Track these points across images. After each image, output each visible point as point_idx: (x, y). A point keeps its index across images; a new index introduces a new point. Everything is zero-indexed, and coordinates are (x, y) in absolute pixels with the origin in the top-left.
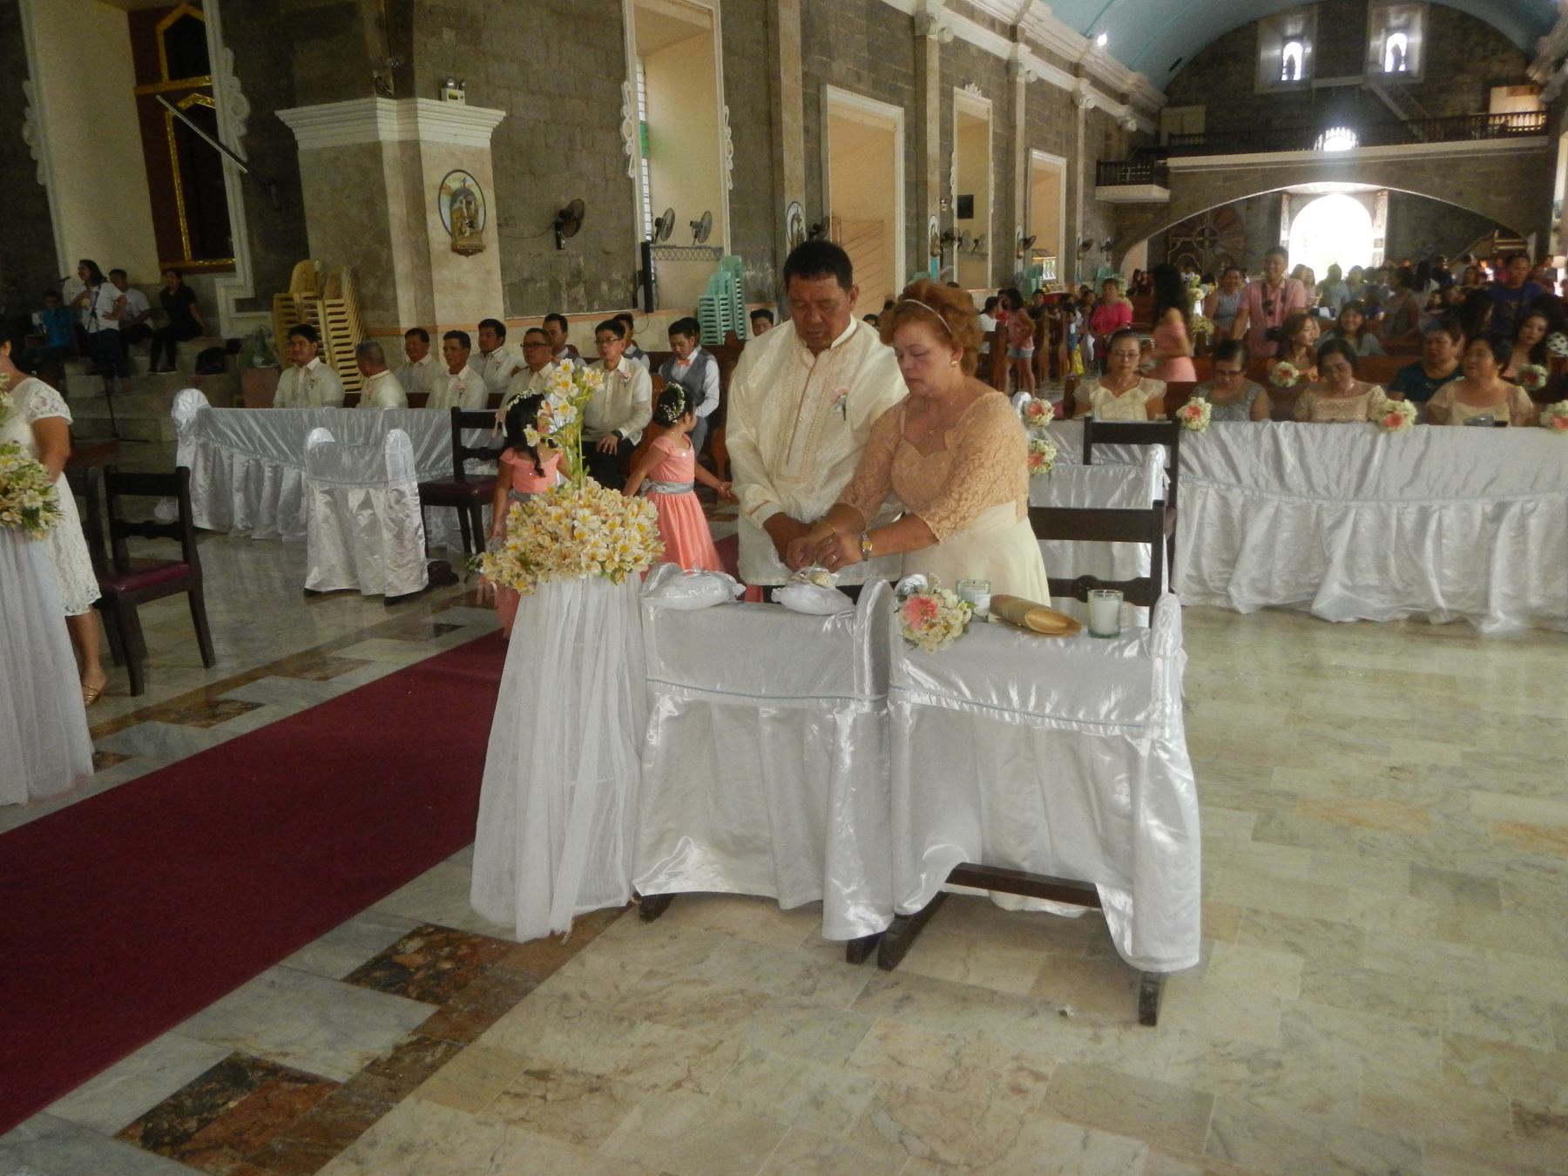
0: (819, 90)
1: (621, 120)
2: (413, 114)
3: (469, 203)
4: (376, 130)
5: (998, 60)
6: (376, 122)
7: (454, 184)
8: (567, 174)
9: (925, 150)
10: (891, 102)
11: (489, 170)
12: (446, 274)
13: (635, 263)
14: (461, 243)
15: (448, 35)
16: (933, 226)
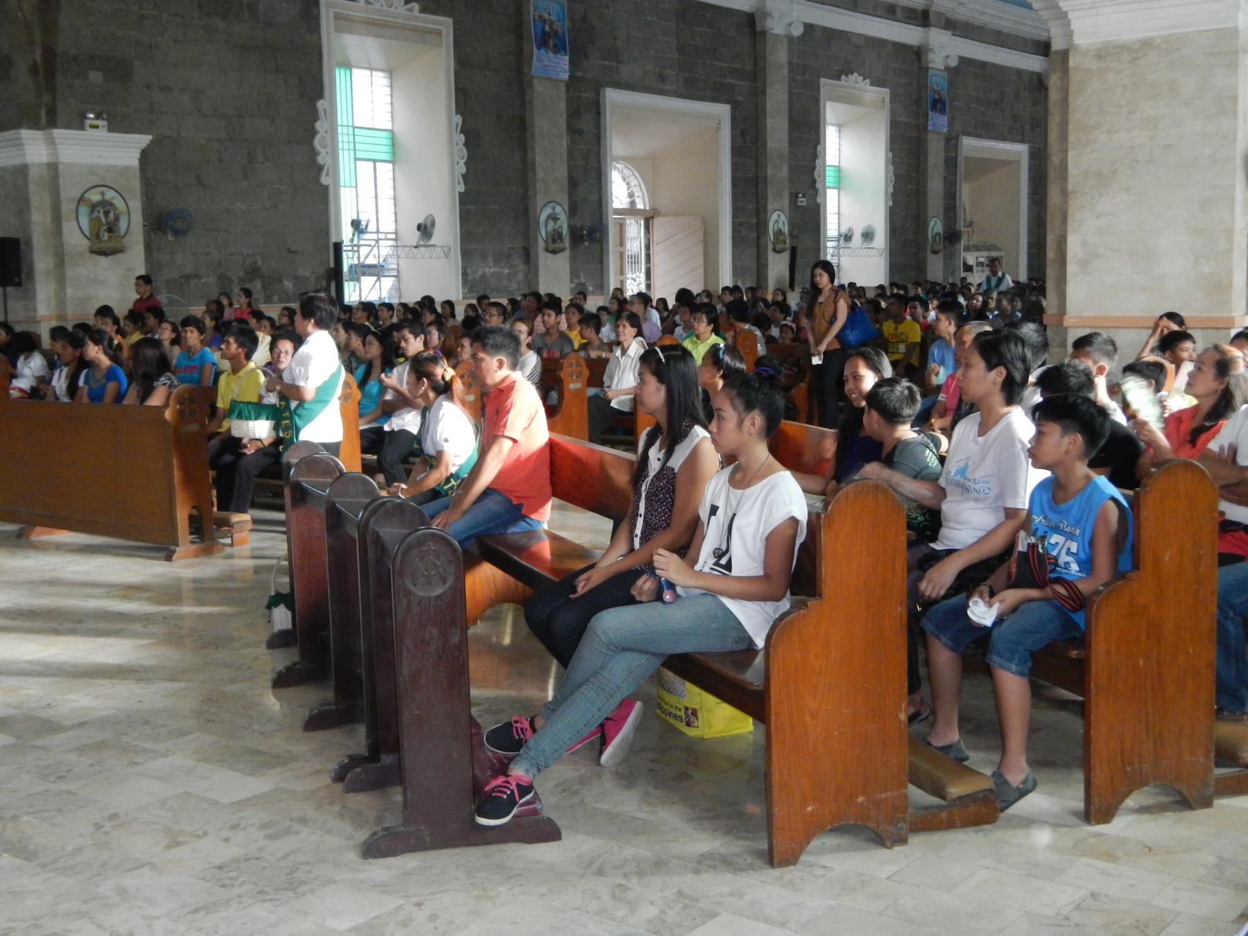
0: (598, 94)
1: (313, 133)
2: (52, 142)
3: (106, 213)
4: (24, 155)
5: (900, 48)
6: (23, 149)
7: (95, 197)
8: (244, 184)
9: (765, 144)
10: (713, 100)
11: (136, 185)
12: (82, 271)
13: (329, 260)
14: (103, 246)
15: (95, 77)
16: (777, 221)
